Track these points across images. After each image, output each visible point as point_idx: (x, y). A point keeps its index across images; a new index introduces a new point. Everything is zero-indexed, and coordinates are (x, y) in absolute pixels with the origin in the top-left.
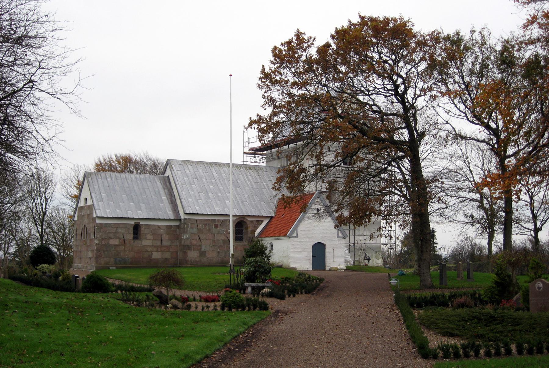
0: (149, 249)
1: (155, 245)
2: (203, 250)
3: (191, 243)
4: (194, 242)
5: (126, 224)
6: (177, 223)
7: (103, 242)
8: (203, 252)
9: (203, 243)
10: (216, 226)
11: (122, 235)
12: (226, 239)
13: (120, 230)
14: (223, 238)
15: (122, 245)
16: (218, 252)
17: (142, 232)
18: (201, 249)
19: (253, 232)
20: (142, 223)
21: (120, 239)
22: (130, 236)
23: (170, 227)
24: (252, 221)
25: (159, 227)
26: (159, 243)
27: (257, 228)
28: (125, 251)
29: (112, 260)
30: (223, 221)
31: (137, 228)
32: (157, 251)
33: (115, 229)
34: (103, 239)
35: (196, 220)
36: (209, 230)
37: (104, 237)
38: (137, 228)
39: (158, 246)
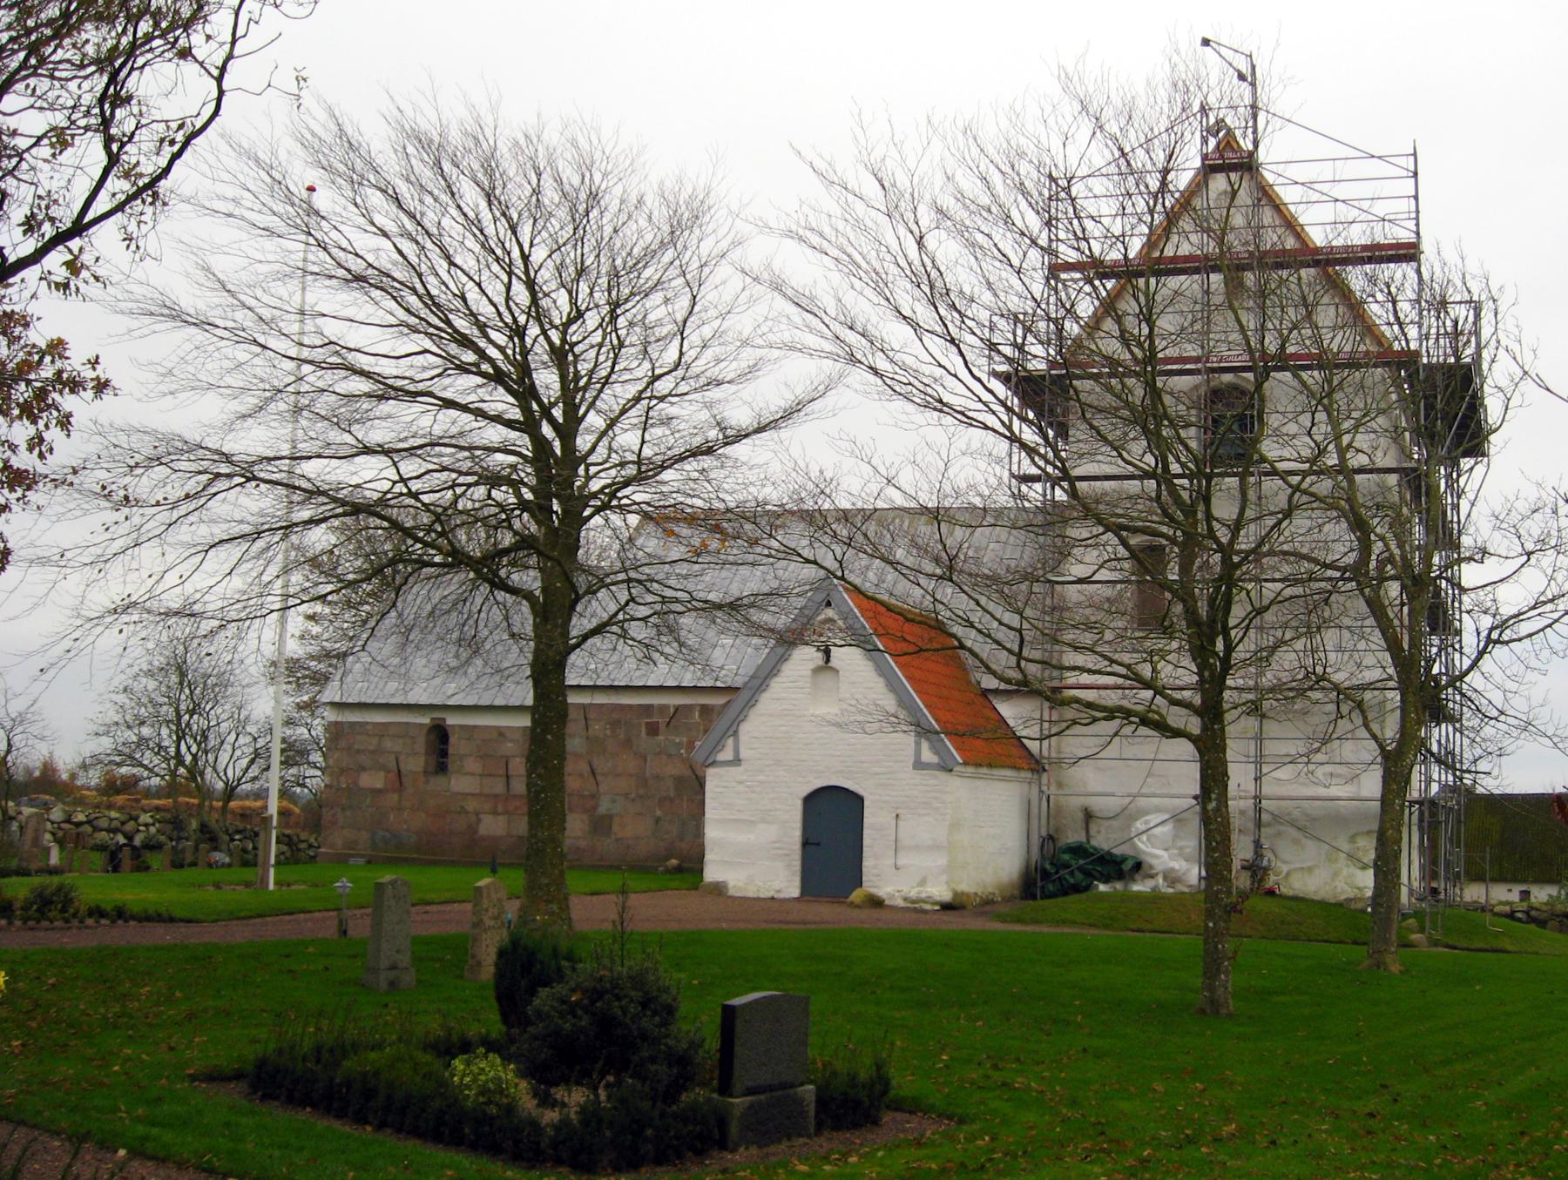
0: (471, 805)
7: (343, 779)
9: (603, 788)
10: (653, 730)
11: (392, 758)
12: (688, 773)
13: (388, 744)
15: (394, 791)
16: (658, 820)
18: (595, 808)
20: (452, 720)
22: (415, 763)
25: (501, 733)
26: (499, 787)
29: (364, 836)
30: (677, 708)
31: (440, 736)
32: (495, 813)
33: (375, 741)
34: (343, 771)
36: (628, 743)
39: (497, 796)
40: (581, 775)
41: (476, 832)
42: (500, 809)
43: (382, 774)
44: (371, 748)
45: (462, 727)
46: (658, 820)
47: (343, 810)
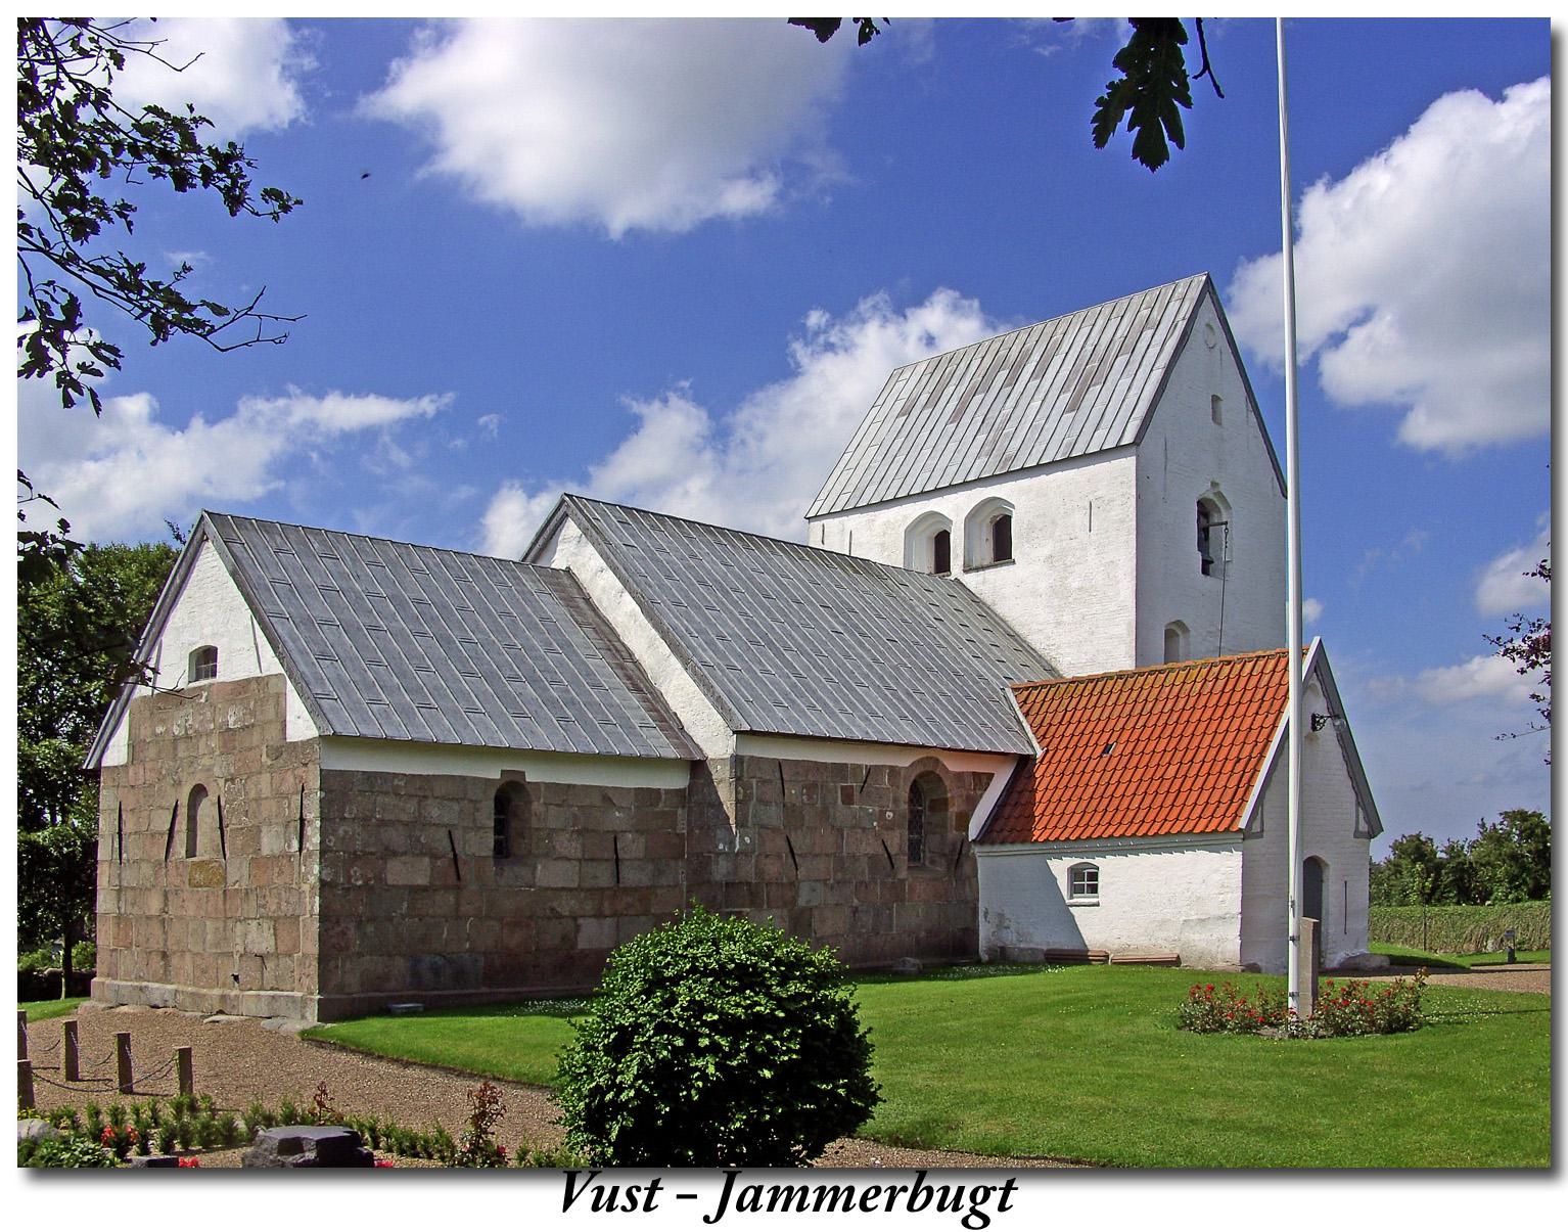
0: (566, 905)
1: (587, 885)
2: (802, 902)
3: (760, 873)
4: (772, 869)
5: (463, 778)
6: (678, 781)
7: (356, 871)
8: (803, 911)
10: (848, 798)
11: (442, 833)
12: (881, 850)
13: (434, 812)
14: (870, 850)
15: (446, 888)
16: (855, 911)
17: (534, 823)
18: (794, 900)
19: (964, 820)
20: (533, 775)
21: (434, 857)
22: (481, 843)
23: (649, 796)
24: (959, 776)
25: (606, 796)
26: (603, 877)
27: (972, 802)
28: (458, 917)
29: (400, 964)
30: (869, 770)
31: (509, 797)
32: (599, 915)
33: (412, 806)
34: (355, 857)
35: (780, 764)
36: (824, 813)
37: (358, 845)
38: (509, 797)
39: (602, 890)
40: (779, 856)
41: (574, 945)
42: (607, 908)
43: (427, 859)
44: (404, 818)
45: (548, 785)
46: (855, 911)
47: (360, 925)
